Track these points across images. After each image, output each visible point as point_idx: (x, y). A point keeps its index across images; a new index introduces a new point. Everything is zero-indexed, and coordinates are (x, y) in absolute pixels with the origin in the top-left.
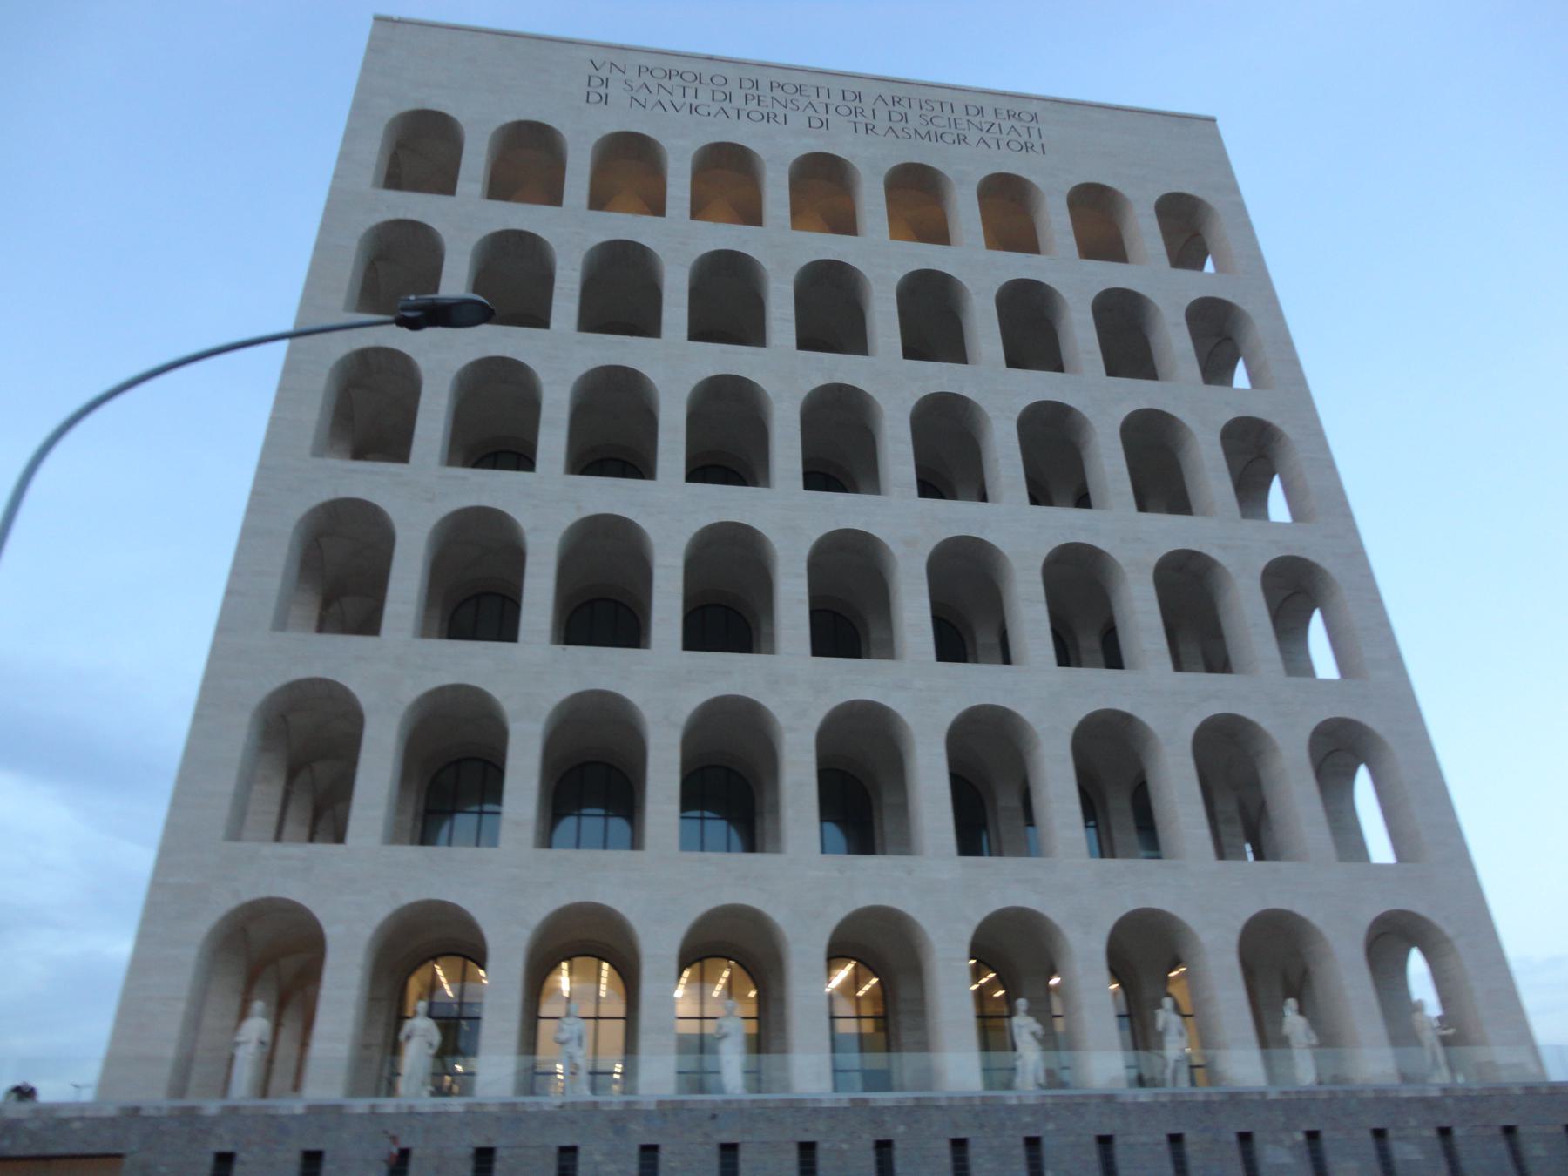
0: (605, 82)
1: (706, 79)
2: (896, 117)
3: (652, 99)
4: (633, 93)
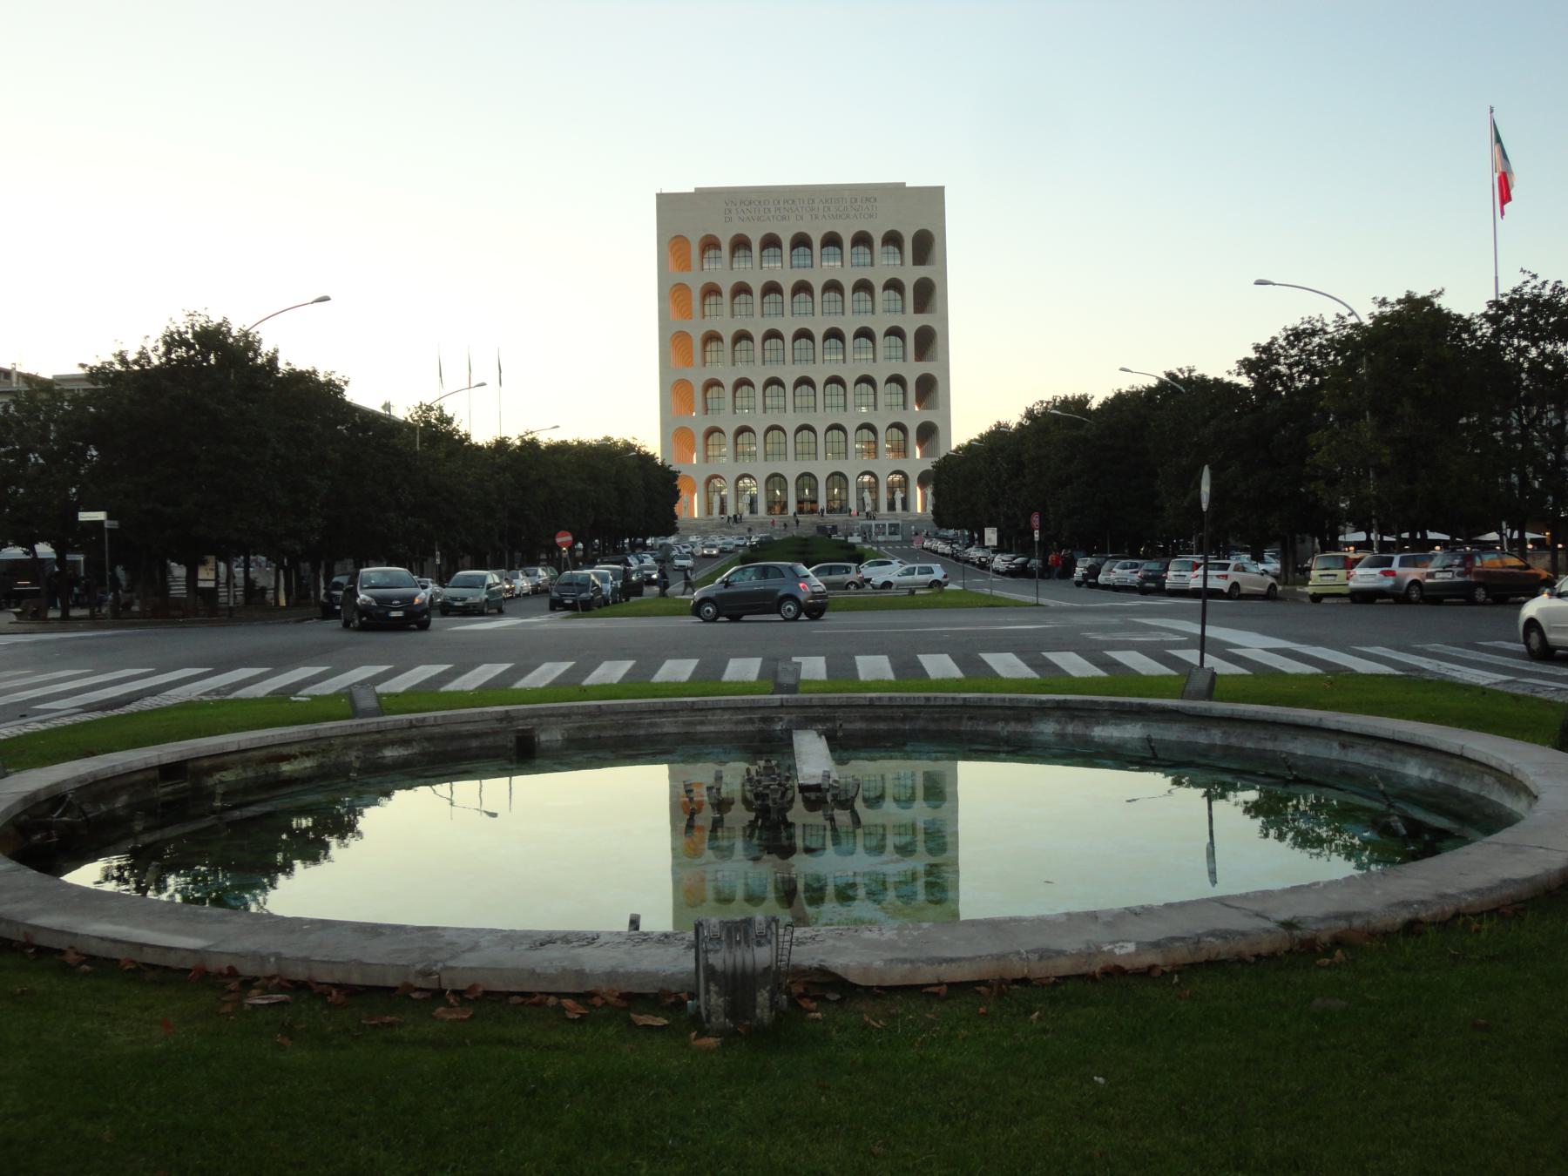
2: (826, 209)
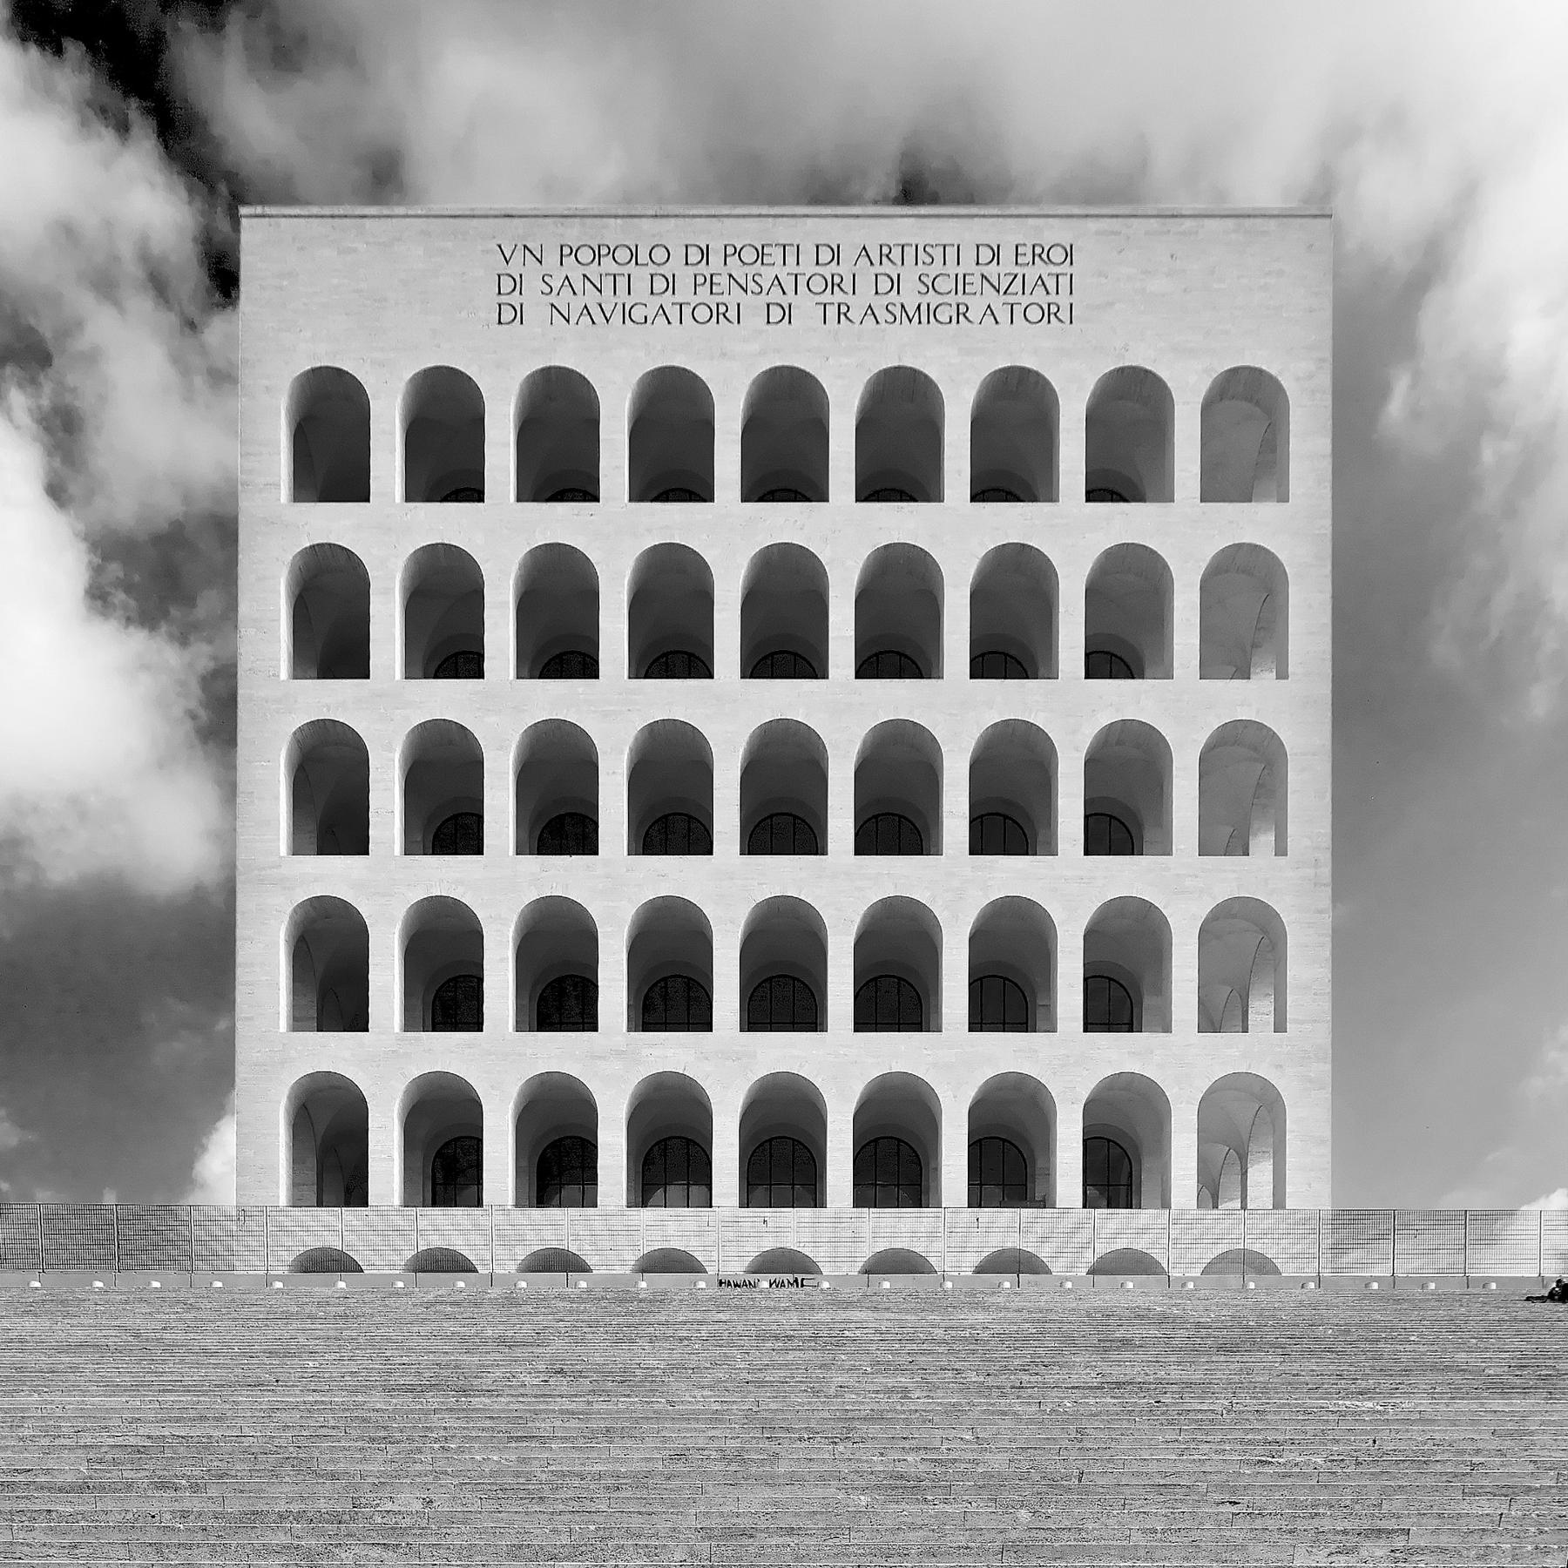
0: (517, 285)
1: (643, 257)
2: (884, 285)
3: (577, 304)
4: (553, 299)
